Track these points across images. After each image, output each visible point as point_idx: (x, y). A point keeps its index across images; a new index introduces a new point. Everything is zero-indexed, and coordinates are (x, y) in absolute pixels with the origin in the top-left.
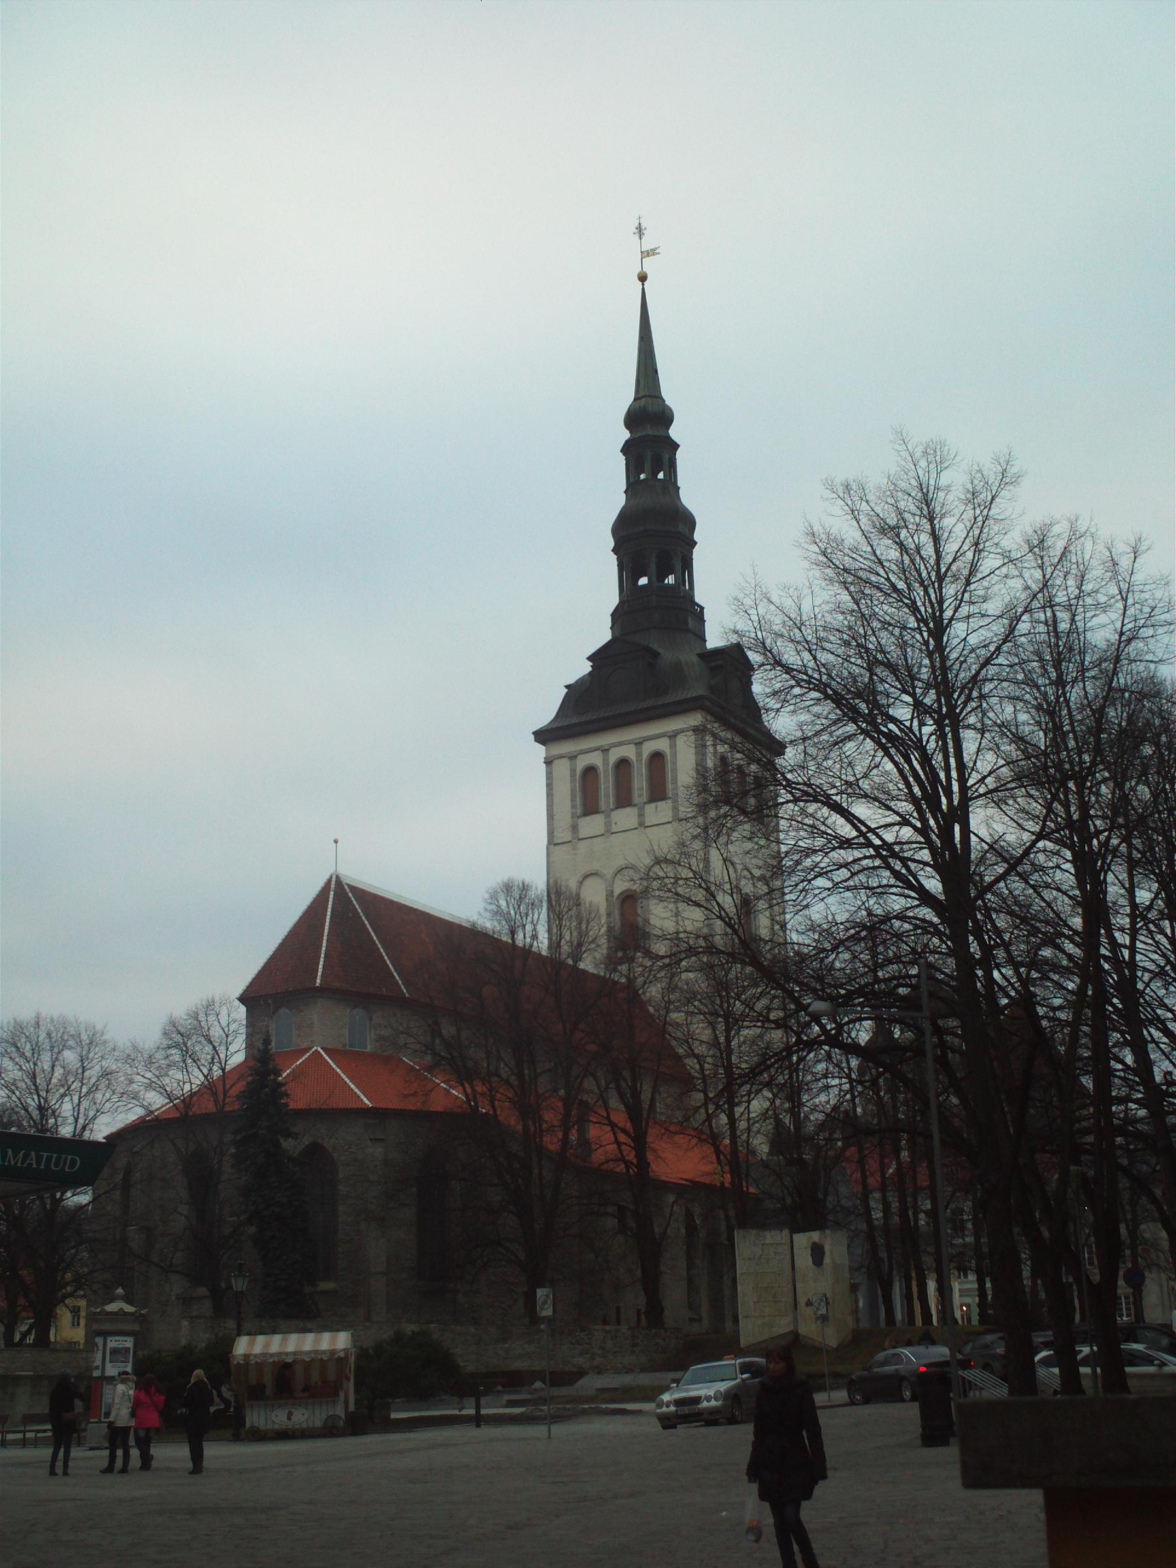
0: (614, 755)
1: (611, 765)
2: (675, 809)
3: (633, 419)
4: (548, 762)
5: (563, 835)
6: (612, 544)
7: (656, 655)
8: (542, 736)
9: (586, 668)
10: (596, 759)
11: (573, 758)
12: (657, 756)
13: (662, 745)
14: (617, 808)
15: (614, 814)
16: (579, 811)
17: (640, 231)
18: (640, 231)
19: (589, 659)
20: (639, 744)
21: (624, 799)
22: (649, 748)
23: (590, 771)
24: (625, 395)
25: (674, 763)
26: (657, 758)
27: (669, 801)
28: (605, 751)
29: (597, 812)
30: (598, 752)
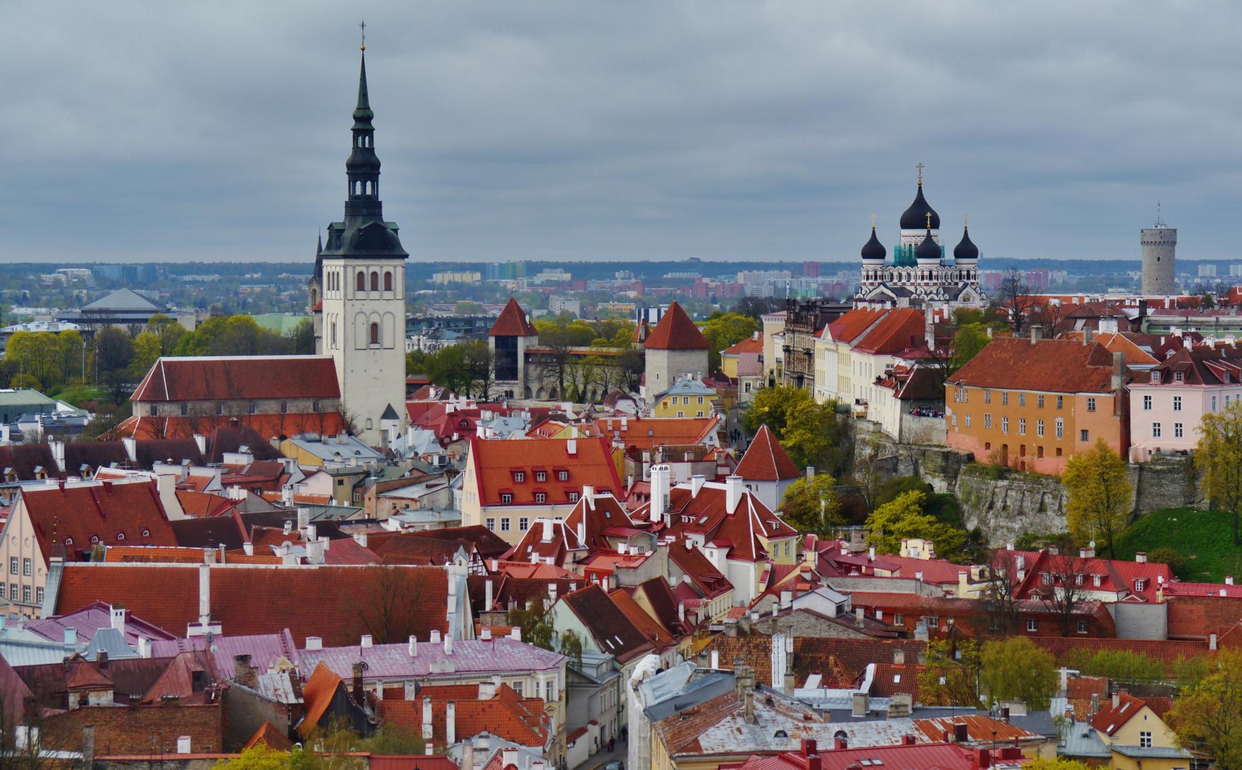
0: (372, 269)
2: (395, 295)
10: (364, 269)
11: (354, 267)
12: (388, 274)
21: (374, 287)
22: (385, 269)
23: (361, 274)
28: (368, 267)
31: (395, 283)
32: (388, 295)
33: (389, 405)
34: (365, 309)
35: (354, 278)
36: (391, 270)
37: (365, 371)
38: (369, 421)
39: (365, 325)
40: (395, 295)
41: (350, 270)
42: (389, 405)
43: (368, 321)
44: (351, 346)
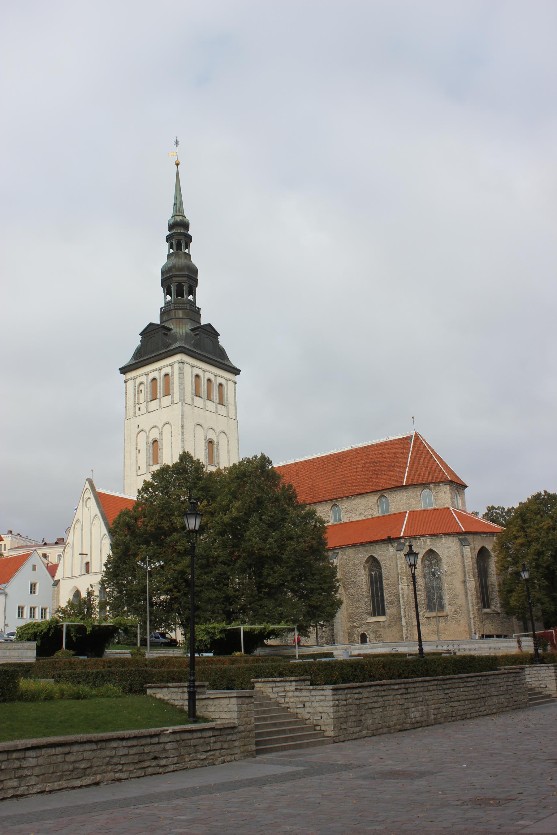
0: (151, 376)
3: (171, 227)
4: (126, 382)
5: (131, 413)
7: (170, 330)
8: (124, 370)
9: (140, 338)
10: (143, 379)
11: (135, 379)
12: (167, 375)
14: (151, 401)
17: (177, 143)
18: (177, 143)
25: (173, 379)
27: (170, 396)
28: (147, 375)
32: (166, 401)
36: (168, 370)
41: (130, 384)
43: (148, 437)
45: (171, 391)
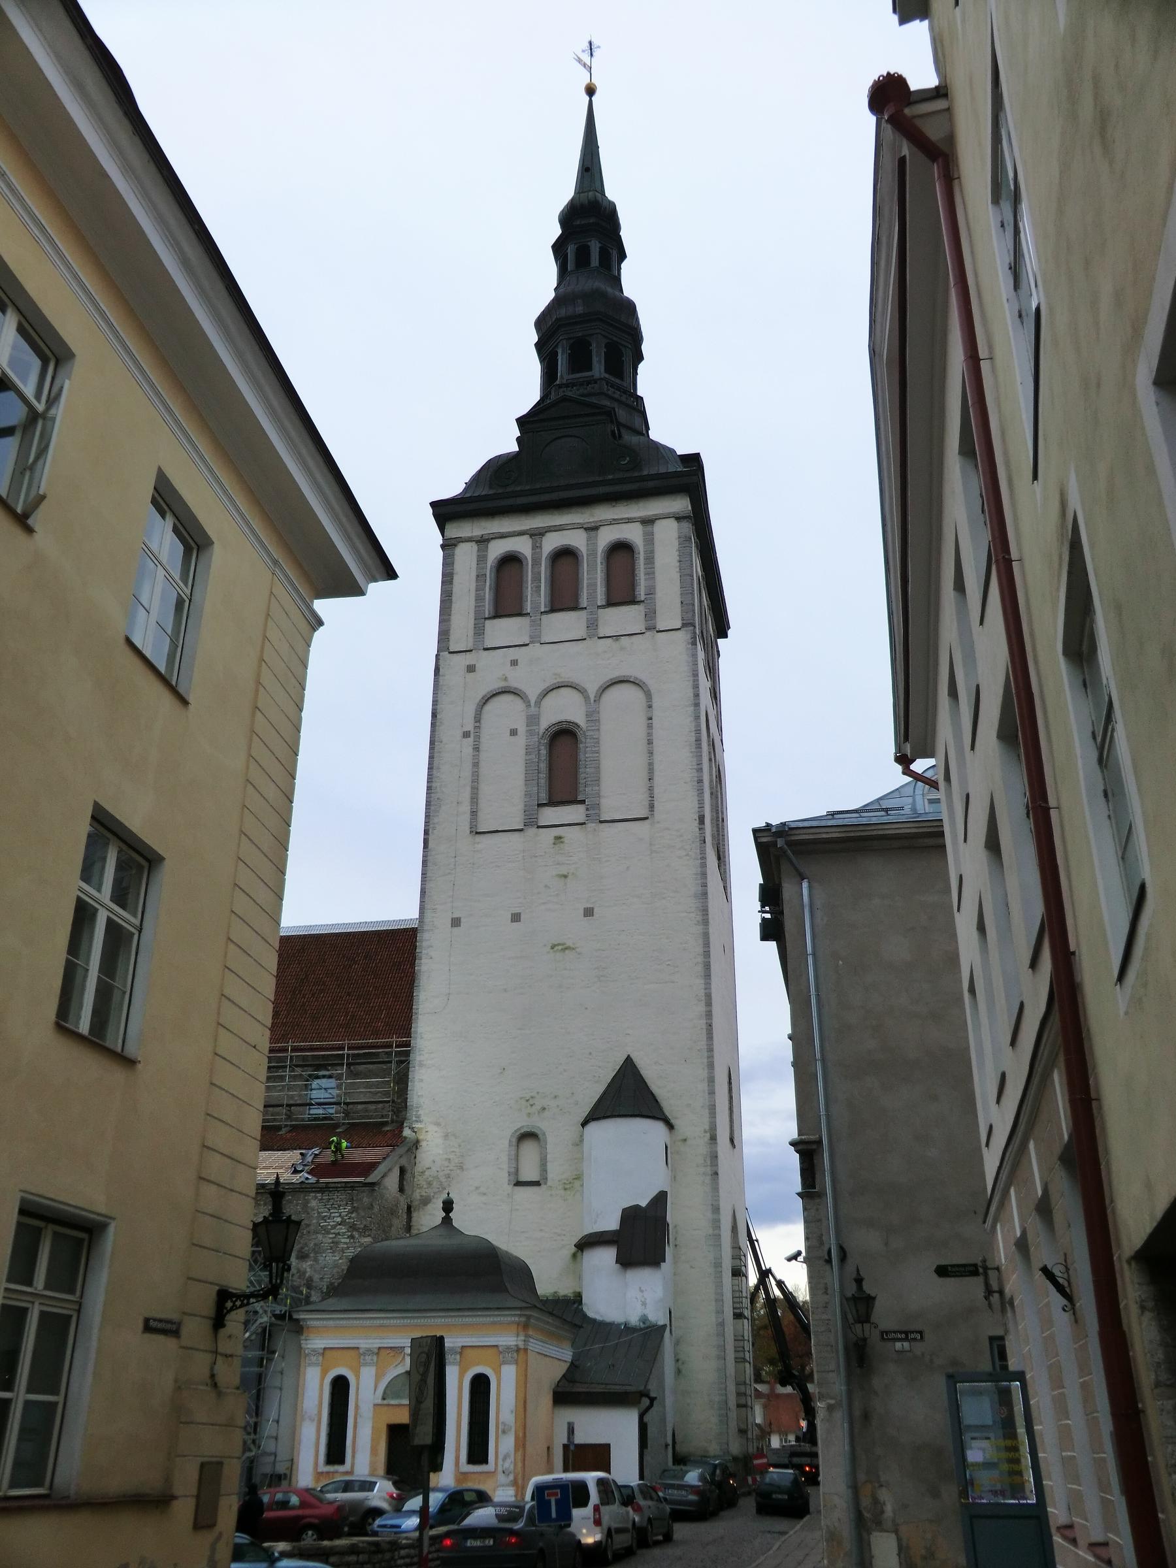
0: (552, 543)
1: (544, 559)
6: (535, 338)
10: (522, 546)
11: (483, 541)
13: (633, 534)
15: (544, 617)
16: (488, 609)
19: (521, 422)
20: (593, 529)
23: (510, 560)
24: (565, 191)
26: (620, 549)
28: (536, 535)
29: (520, 614)
30: (526, 538)
31: (651, 574)
33: (629, 1064)
34: (516, 679)
35: (480, 577)
37: (516, 918)
38: (529, 1148)
39: (521, 740)
40: (650, 615)
42: (629, 1064)
43: (533, 720)
44: (456, 816)
45: (641, 593)
